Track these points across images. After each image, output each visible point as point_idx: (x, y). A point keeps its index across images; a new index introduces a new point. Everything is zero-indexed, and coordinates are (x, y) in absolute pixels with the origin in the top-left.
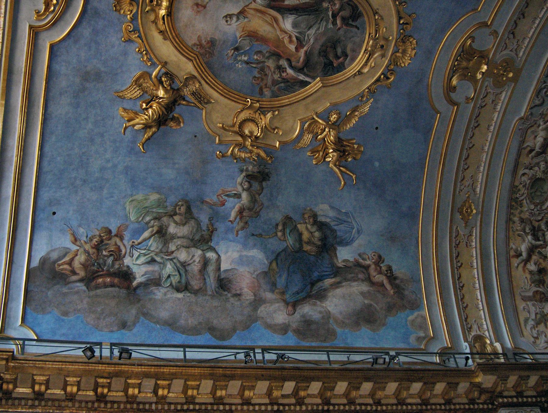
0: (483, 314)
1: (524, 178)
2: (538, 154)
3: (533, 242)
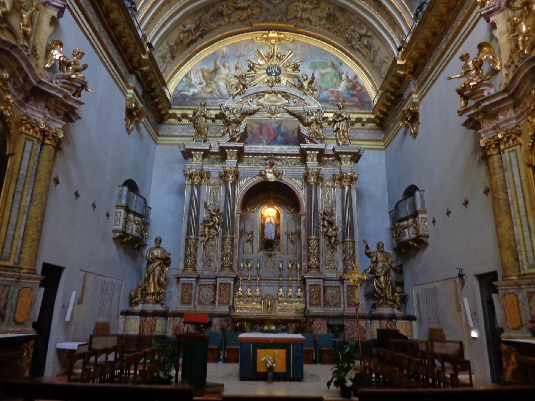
0: (155, 30)
1: (221, 7)
2: (235, 8)
3: (193, 29)
